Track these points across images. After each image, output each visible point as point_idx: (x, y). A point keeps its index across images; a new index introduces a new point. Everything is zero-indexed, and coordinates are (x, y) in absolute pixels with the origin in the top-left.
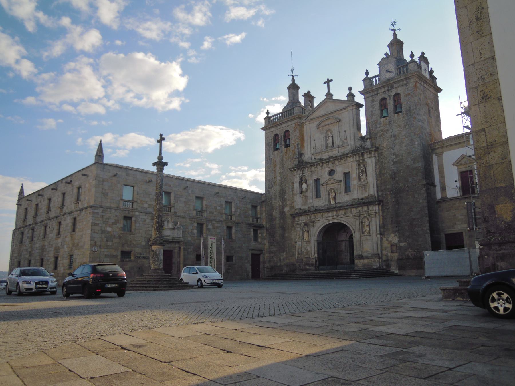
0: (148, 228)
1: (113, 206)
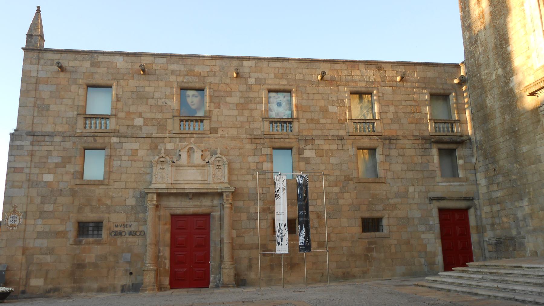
0: (143, 169)
1: (60, 129)
